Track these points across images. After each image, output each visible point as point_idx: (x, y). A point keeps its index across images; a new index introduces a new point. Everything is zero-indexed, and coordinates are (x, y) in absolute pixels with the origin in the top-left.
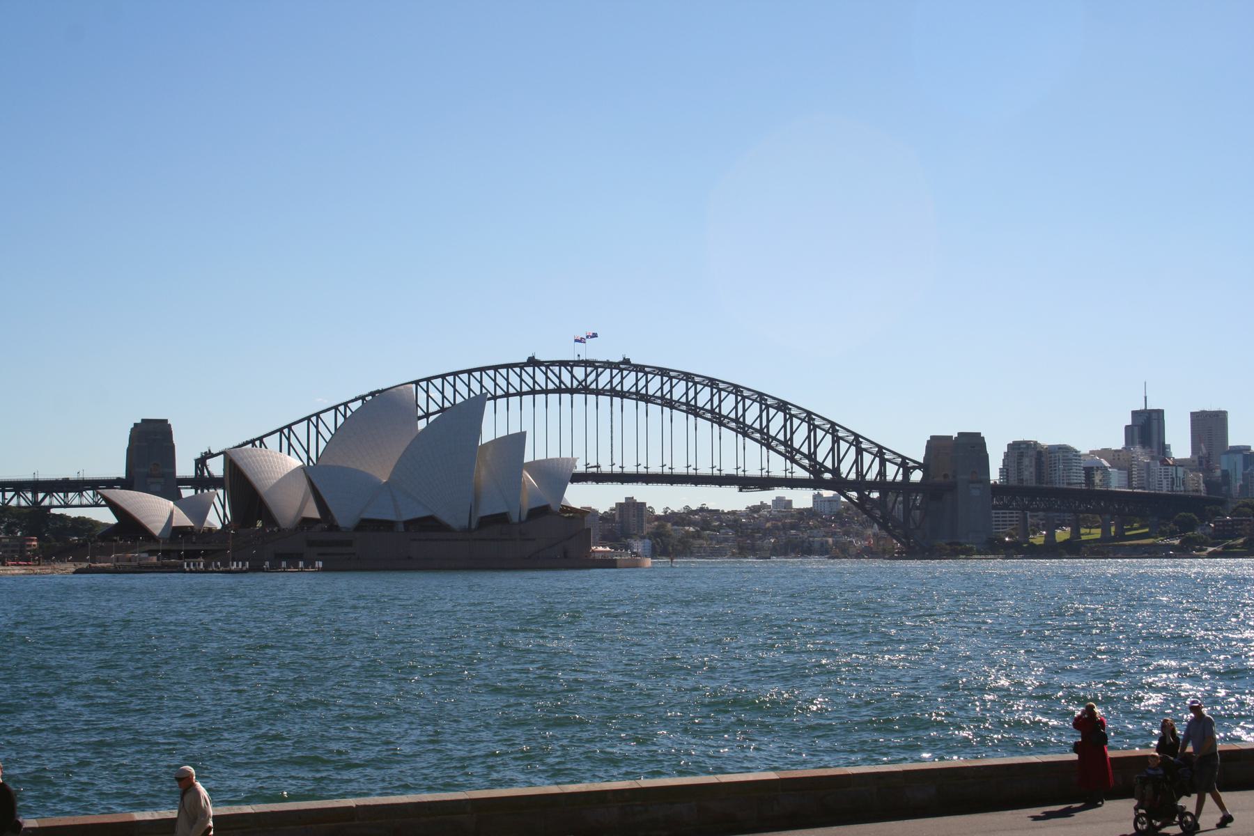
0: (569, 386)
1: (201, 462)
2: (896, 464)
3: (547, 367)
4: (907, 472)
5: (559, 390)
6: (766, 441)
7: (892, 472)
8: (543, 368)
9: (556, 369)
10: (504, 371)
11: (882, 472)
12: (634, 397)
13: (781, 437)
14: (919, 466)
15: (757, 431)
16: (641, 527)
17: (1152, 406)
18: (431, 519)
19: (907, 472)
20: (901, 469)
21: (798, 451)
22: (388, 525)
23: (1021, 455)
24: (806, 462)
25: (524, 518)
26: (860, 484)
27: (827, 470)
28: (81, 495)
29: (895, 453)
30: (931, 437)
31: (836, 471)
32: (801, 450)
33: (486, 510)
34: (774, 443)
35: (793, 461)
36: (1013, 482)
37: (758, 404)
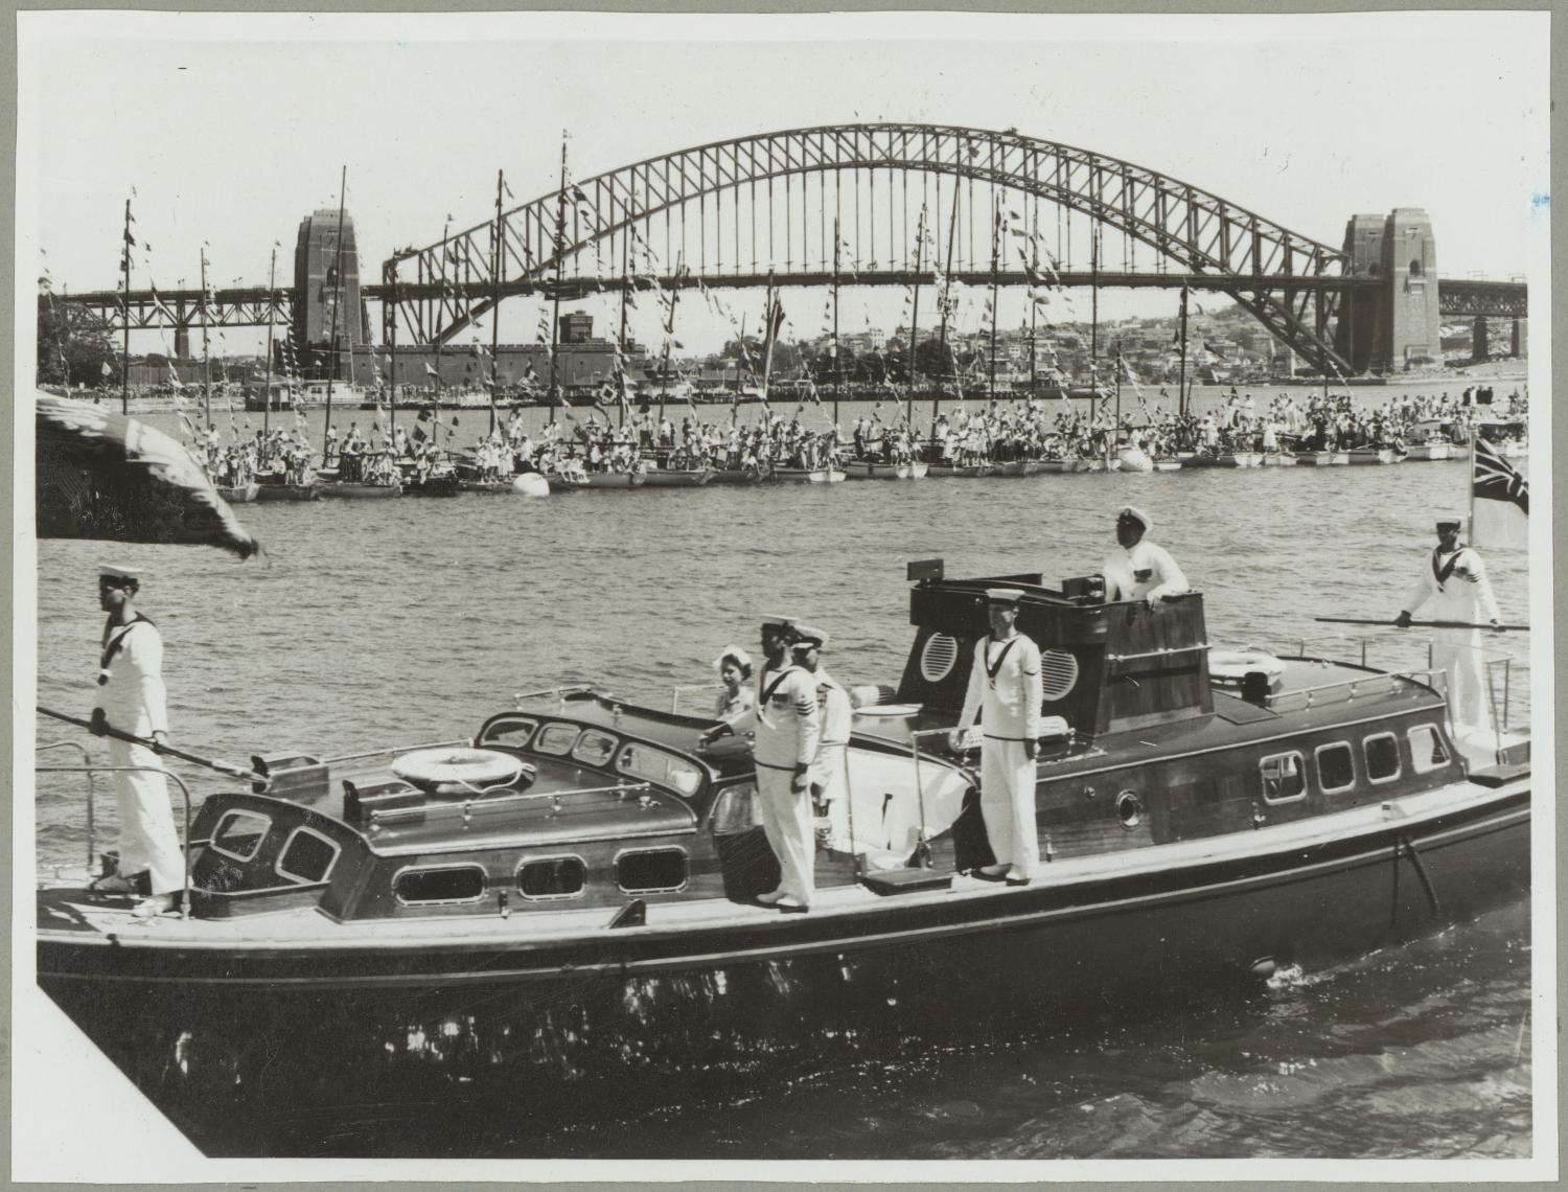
0: (868, 158)
1: (390, 267)
2: (1305, 253)
3: (839, 133)
4: (1321, 263)
5: (856, 164)
6: (1131, 228)
8: (834, 135)
9: (851, 136)
10: (781, 141)
11: (1287, 263)
12: (955, 170)
13: (1151, 220)
15: (1118, 212)
19: (1321, 263)
20: (1313, 262)
21: (1174, 238)
24: (1184, 253)
26: (1259, 282)
28: (239, 309)
29: (1305, 239)
31: (1223, 264)
32: (1178, 236)
34: (1141, 229)
35: (1166, 251)
37: (1120, 178)
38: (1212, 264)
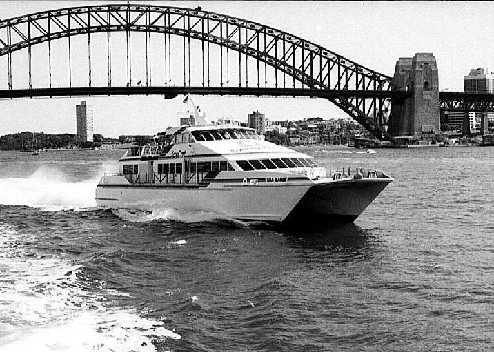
14: (389, 79)
31: (321, 84)
35: (295, 77)
38: (317, 83)
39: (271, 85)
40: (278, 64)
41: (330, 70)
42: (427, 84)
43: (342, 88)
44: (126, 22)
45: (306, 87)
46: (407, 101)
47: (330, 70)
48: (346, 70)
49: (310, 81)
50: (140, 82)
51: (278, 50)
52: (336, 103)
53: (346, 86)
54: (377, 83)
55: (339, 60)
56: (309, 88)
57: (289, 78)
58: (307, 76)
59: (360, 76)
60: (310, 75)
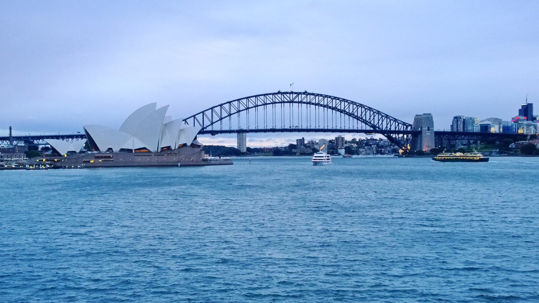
0: (289, 100)
3: (281, 94)
7: (402, 128)
14: (411, 125)
16: (343, 145)
17: (530, 102)
18: (145, 148)
22: (130, 151)
23: (457, 121)
25: (176, 148)
27: (377, 127)
30: (416, 115)
31: (379, 128)
33: (164, 145)
35: (366, 124)
36: (455, 130)
39: (355, 128)
40: (357, 118)
41: (382, 121)
42: (428, 127)
43: (388, 129)
44: (293, 99)
45: (372, 129)
46: (419, 135)
47: (382, 121)
48: (390, 121)
49: (374, 126)
50: (297, 127)
51: (359, 112)
52: (385, 136)
53: (390, 128)
54: (405, 127)
55: (387, 116)
56: (373, 129)
57: (364, 124)
58: (372, 124)
59: (397, 124)
60: (373, 124)
